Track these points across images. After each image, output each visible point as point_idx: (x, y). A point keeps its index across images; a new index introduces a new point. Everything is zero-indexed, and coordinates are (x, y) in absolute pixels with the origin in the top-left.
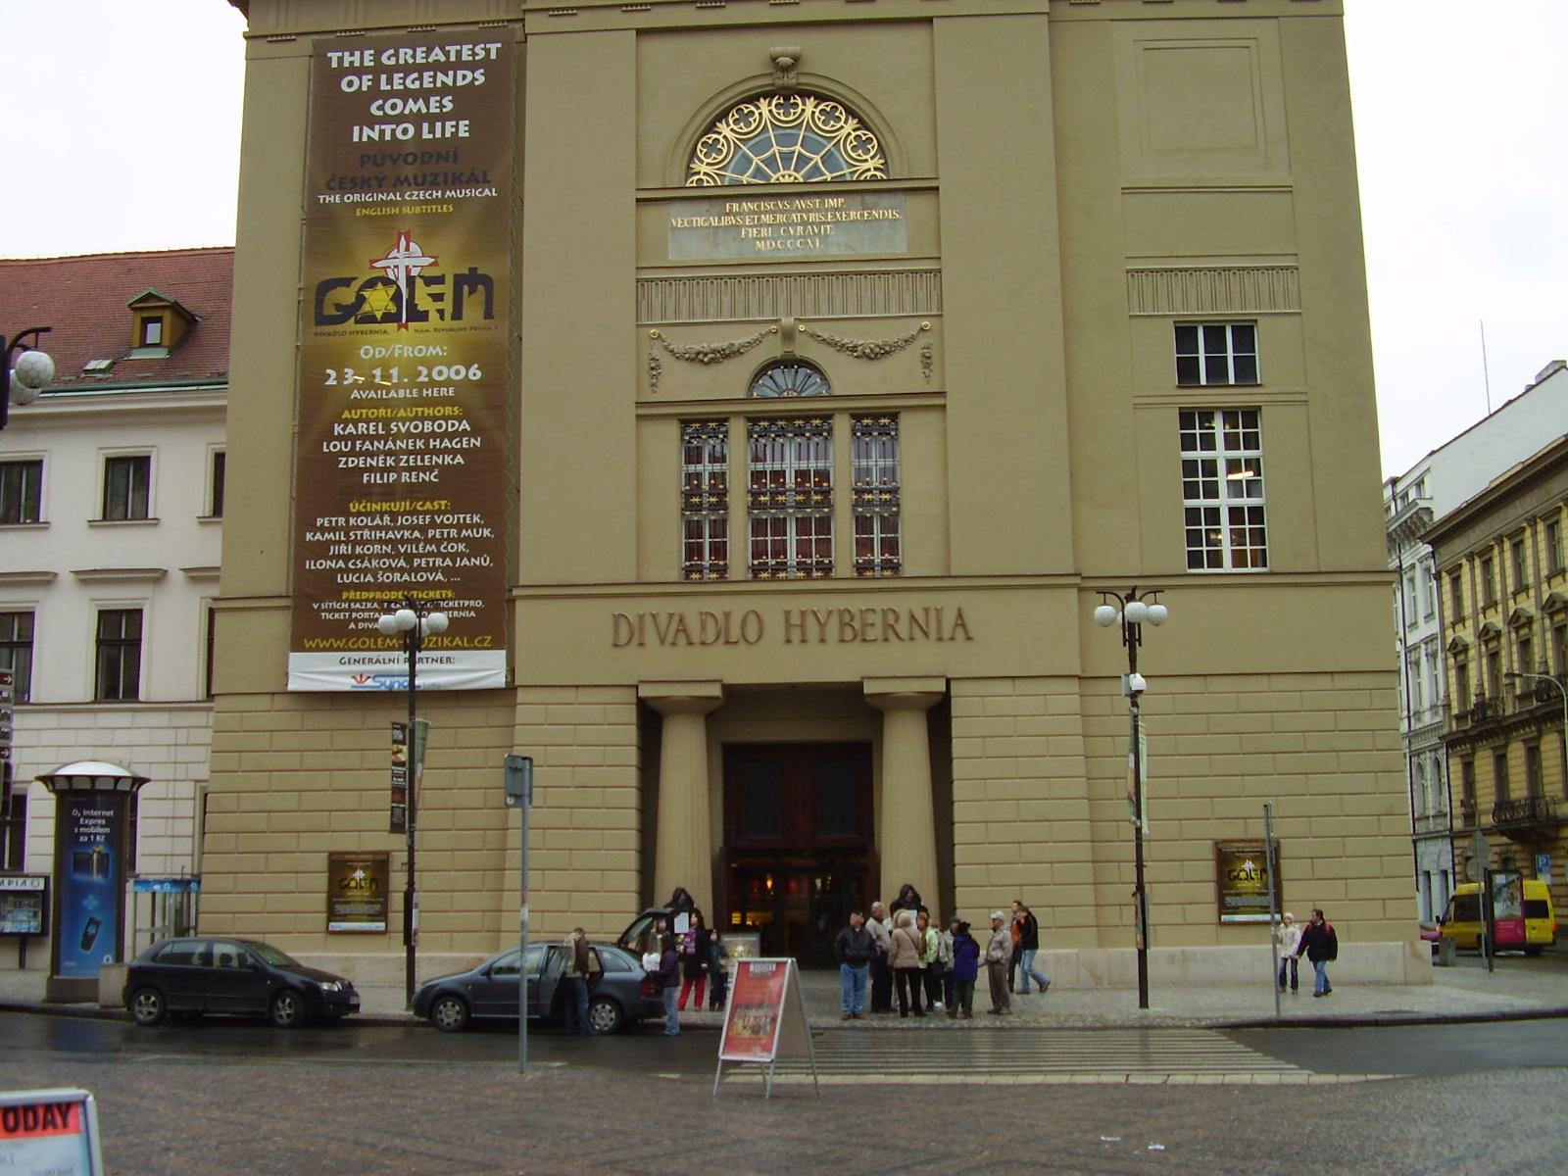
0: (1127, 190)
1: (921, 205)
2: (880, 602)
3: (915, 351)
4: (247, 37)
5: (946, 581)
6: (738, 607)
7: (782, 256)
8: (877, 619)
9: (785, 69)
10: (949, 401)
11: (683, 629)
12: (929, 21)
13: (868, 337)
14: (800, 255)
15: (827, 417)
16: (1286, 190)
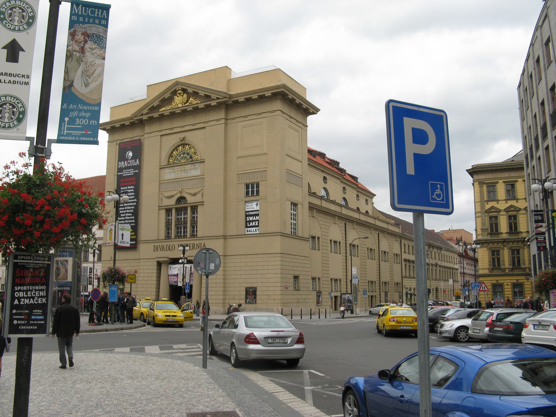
0: (238, 158)
1: (202, 164)
2: (192, 242)
3: (201, 193)
4: (108, 142)
5: (203, 238)
6: (171, 244)
7: (181, 177)
8: (191, 245)
9: (182, 140)
10: (205, 203)
11: (163, 248)
12: (205, 127)
13: (193, 191)
14: (184, 176)
15: (187, 208)
16: (266, 154)
